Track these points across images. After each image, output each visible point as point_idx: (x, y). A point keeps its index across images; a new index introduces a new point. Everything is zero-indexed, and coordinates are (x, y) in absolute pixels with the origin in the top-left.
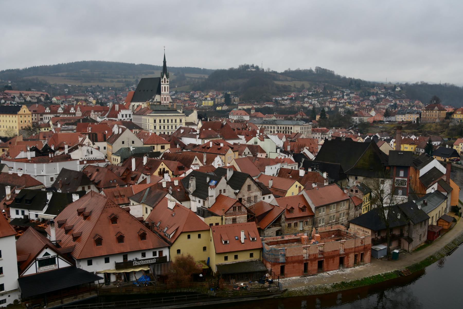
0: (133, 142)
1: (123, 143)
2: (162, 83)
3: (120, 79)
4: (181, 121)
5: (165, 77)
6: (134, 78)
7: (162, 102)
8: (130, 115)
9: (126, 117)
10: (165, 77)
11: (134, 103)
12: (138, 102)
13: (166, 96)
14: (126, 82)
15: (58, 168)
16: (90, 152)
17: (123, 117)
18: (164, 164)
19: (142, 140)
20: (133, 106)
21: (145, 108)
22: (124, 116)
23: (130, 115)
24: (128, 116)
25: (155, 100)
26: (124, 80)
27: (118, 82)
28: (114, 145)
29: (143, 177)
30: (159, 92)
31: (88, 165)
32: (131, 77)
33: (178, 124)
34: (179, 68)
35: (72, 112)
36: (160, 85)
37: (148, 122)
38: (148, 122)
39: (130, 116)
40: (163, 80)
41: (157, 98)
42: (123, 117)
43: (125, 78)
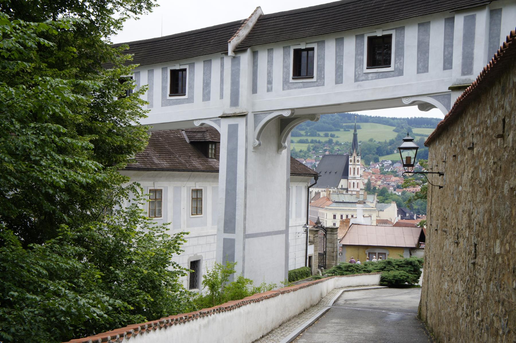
2: (350, 163)
3: (304, 138)
5: (354, 154)
6: (326, 135)
7: (349, 189)
10: (354, 154)
13: (355, 181)
14: (312, 142)
21: (324, 197)
25: (340, 186)
26: (310, 139)
27: (301, 142)
32: (322, 134)
34: (404, 119)
36: (347, 165)
37: (325, 217)
38: (325, 217)
41: (343, 183)
43: (312, 135)
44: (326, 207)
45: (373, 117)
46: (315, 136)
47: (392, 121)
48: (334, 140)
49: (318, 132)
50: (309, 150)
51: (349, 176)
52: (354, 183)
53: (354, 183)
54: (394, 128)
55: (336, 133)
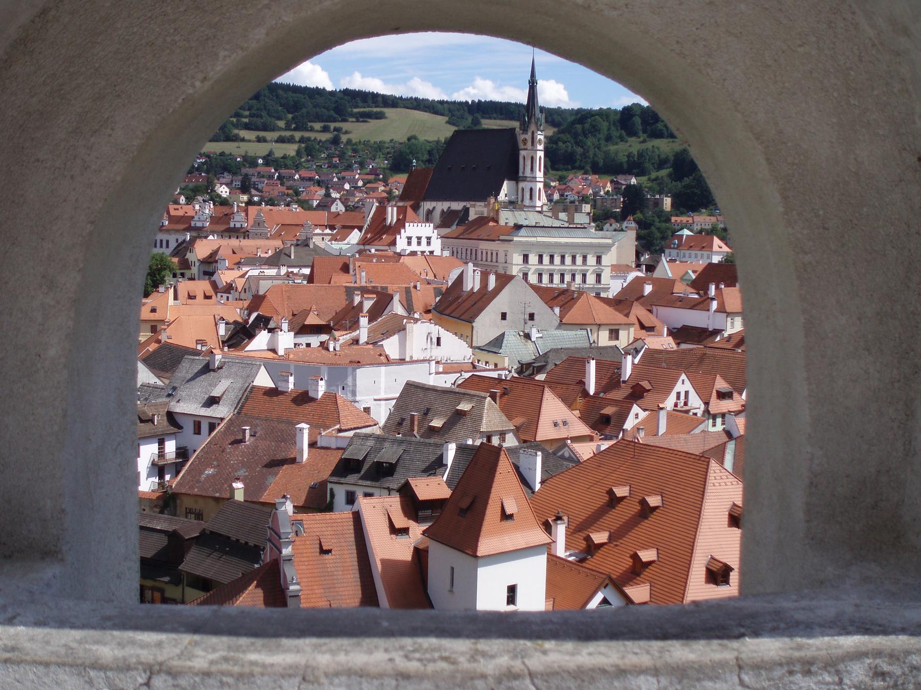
0: (532, 317)
1: (504, 316)
2: (521, 146)
3: (287, 134)
4: (599, 259)
6: (325, 129)
8: (429, 238)
9: (419, 243)
11: (434, 204)
12: (446, 200)
14: (302, 140)
15: (383, 379)
16: (435, 340)
17: (409, 243)
18: (687, 382)
19: (557, 310)
20: (430, 213)
22: (414, 241)
23: (429, 238)
24: (424, 241)
26: (298, 135)
28: (479, 322)
29: (637, 416)
30: (514, 174)
31: (467, 375)
32: (318, 126)
33: (591, 269)
34: (461, 103)
35: (238, 225)
39: (429, 243)
40: (528, 136)
42: (409, 243)
44: (502, 237)
45: (407, 99)
46: (306, 129)
47: (440, 106)
48: (344, 138)
49: (310, 124)
50: (298, 152)
51: (521, 174)
52: (531, 189)
53: (531, 189)
54: (446, 119)
55: (345, 126)
